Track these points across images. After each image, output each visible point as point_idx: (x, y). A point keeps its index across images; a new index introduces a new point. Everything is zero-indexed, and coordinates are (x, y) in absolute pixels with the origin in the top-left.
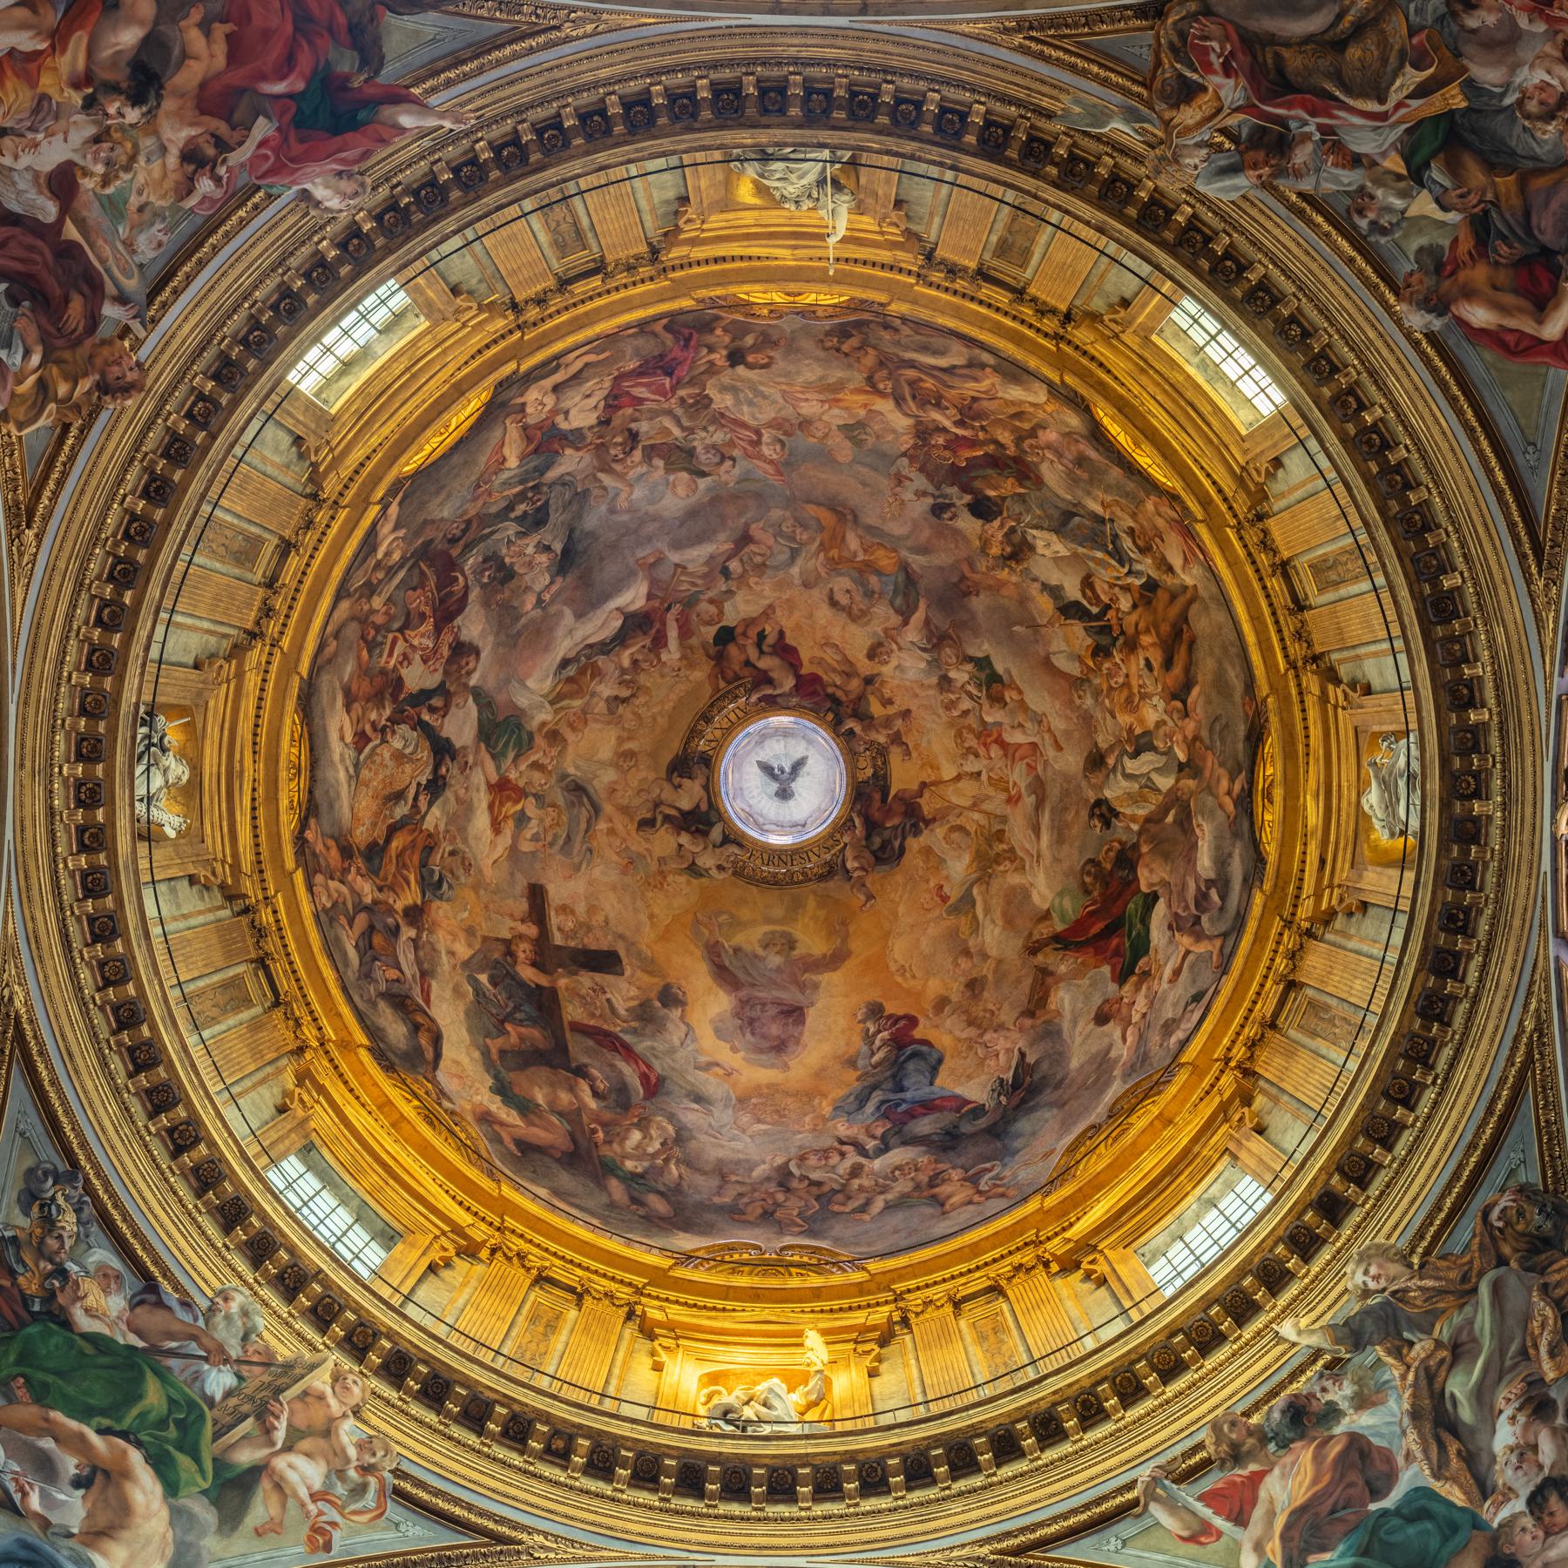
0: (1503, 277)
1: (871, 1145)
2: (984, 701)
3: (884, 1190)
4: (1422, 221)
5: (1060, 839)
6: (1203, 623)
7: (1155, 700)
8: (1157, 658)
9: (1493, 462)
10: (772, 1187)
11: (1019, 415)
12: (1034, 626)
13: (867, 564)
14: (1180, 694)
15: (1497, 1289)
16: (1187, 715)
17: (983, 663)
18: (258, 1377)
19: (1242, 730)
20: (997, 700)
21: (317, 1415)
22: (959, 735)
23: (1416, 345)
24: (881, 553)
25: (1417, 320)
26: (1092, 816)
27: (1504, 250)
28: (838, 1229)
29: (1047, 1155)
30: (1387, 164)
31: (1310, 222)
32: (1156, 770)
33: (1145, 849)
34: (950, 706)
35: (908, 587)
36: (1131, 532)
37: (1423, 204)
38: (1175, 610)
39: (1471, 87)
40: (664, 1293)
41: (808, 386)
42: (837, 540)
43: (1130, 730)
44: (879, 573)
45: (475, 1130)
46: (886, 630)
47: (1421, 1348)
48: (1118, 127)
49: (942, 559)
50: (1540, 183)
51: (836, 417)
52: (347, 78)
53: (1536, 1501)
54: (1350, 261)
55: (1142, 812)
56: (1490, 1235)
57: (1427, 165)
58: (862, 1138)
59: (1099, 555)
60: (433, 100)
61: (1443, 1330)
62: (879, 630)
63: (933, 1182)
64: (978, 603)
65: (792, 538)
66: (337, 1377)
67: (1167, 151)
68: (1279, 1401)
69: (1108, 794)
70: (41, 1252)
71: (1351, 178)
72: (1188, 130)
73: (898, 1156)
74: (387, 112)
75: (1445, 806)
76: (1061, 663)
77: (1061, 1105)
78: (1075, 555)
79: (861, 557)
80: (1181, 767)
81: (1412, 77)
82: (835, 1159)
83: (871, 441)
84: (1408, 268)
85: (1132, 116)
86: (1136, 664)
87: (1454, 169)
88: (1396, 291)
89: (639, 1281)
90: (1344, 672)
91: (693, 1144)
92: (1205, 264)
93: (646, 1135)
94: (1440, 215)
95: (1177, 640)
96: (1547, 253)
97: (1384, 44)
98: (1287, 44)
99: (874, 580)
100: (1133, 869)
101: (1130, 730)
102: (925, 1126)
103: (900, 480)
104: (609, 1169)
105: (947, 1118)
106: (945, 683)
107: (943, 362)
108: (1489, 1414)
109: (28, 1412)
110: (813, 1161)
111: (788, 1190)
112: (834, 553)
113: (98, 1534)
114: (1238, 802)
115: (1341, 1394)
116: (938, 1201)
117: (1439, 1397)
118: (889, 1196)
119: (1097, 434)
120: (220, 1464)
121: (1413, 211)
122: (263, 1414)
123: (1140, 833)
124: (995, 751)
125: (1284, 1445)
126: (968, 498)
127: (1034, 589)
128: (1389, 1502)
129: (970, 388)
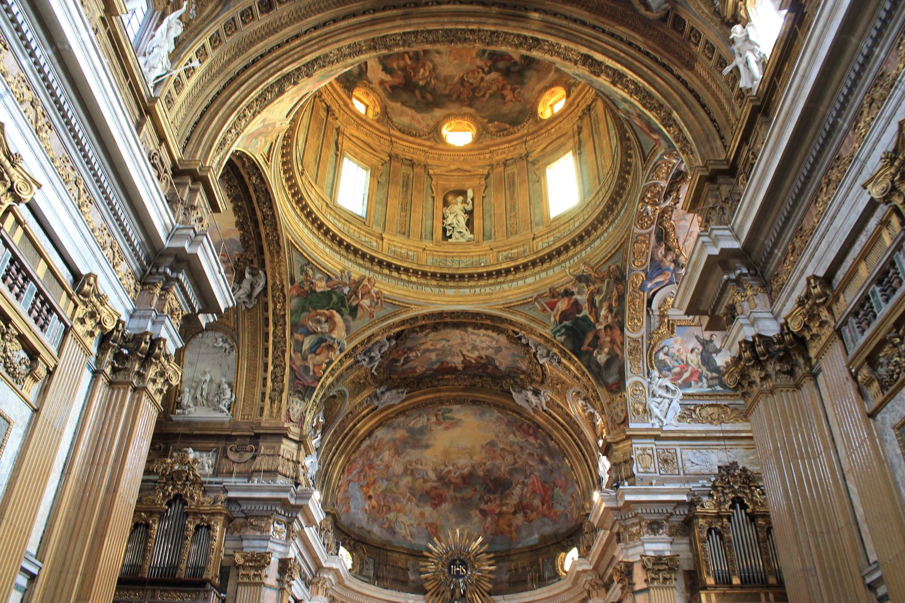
1: (486, 69)
3: (489, 89)
10: (459, 86)
15: (608, 282)
18: (353, 286)
21: (367, 290)
28: (478, 104)
29: (533, 90)
40: (433, 151)
45: (380, 90)
47: (592, 287)
53: (606, 328)
56: (609, 273)
58: (484, 66)
61: (597, 286)
63: (503, 88)
66: (369, 280)
68: (563, 288)
70: (307, 281)
73: (494, 75)
75: (620, 172)
77: (537, 71)
82: (476, 74)
89: (426, 149)
91: (438, 71)
93: (425, 70)
102: (501, 65)
104: (416, 86)
105: (508, 63)
108: (601, 307)
109: (313, 313)
110: (470, 75)
111: (464, 87)
113: (331, 330)
115: (575, 290)
116: (503, 97)
117: (593, 299)
118: (491, 91)
120: (350, 307)
122: (356, 293)
125: (563, 297)
128: (580, 315)
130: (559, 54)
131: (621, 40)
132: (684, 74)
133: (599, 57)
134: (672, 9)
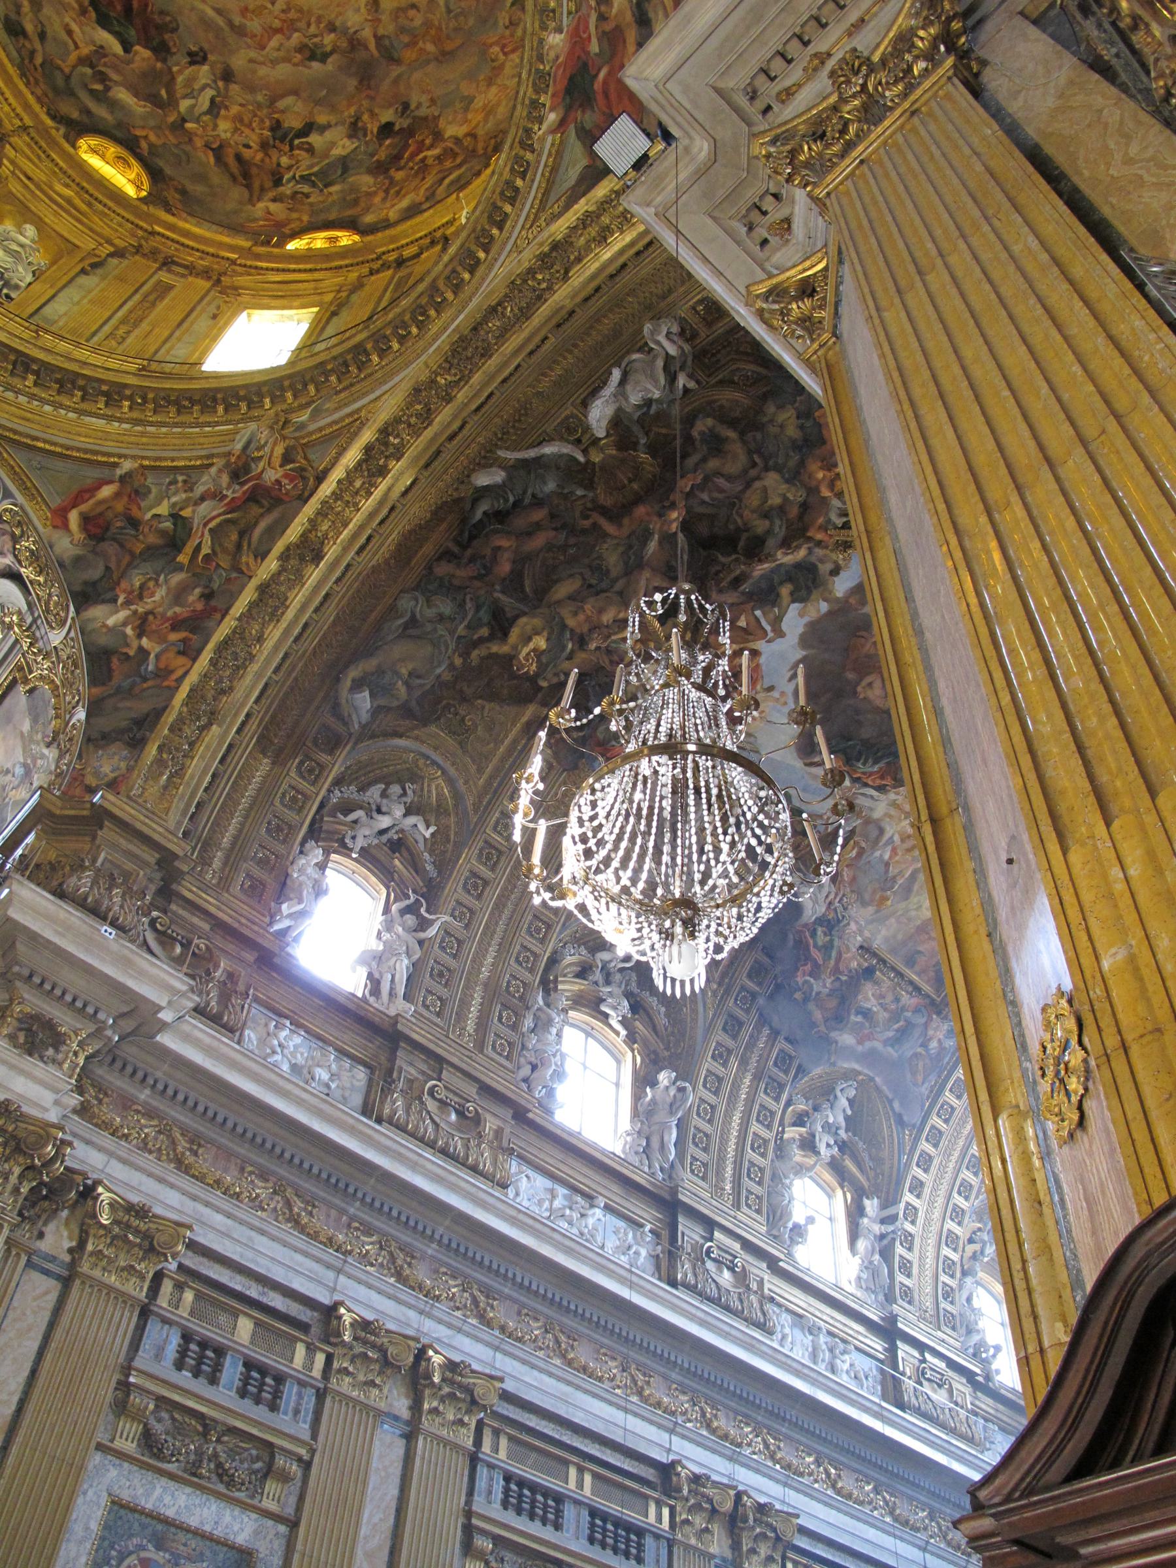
0: (110, 514)
2: (306, 40)
4: (158, 502)
5: (206, 23)
6: (237, 193)
7: (229, 135)
8: (247, 154)
9: (47, 447)
11: (398, 193)
12: (318, 102)
13: (416, 43)
14: (218, 152)
16: (207, 146)
17: (323, 58)
19: (168, 171)
20: (301, 49)
22: (301, 11)
23: (120, 456)
24: (414, 56)
25: (127, 466)
26: (201, 49)
27: (119, 524)
30: (190, 510)
31: (201, 457)
32: (194, 106)
33: (159, 65)
34: (319, 20)
35: (390, 56)
36: (307, 196)
37: (163, 509)
38: (256, 185)
39: (180, 568)
41: (498, 104)
42: (437, 41)
43: (227, 108)
44: (407, 45)
46: (379, 20)
48: (304, 417)
49: (385, 86)
50: (127, 559)
51: (478, 103)
52: (583, 112)
54: (173, 460)
55: (180, 79)
57: (175, 524)
59: (316, 169)
60: (550, 139)
62: (383, 17)
64: (352, 83)
65: (456, 17)
67: (282, 424)
69: (206, 68)
71: (200, 489)
72: (275, 444)
74: (561, 112)
76: (289, 100)
78: (326, 156)
79: (421, 44)
80: (184, 120)
81: (205, 550)
83: (458, 105)
84: (149, 480)
85: (302, 426)
86: (254, 140)
87: (163, 533)
88: (142, 466)
90: (114, 261)
92: (242, 393)
94: (154, 511)
95: (244, 173)
96: (103, 539)
97: (225, 550)
98: (262, 515)
99: (406, 39)
100: (154, 50)
101: (227, 108)
103: (433, 101)
106: (332, 28)
107: (447, 181)
112: (433, 32)
114: (137, 138)
119: (351, 225)
121: (165, 502)
123: (170, 69)
124: (277, 24)
126: (397, 127)
127: (332, 119)
129: (429, 181)
130: (336, 496)
131: (316, 610)
132: (253, 726)
133: (314, 575)
134: (350, 735)
